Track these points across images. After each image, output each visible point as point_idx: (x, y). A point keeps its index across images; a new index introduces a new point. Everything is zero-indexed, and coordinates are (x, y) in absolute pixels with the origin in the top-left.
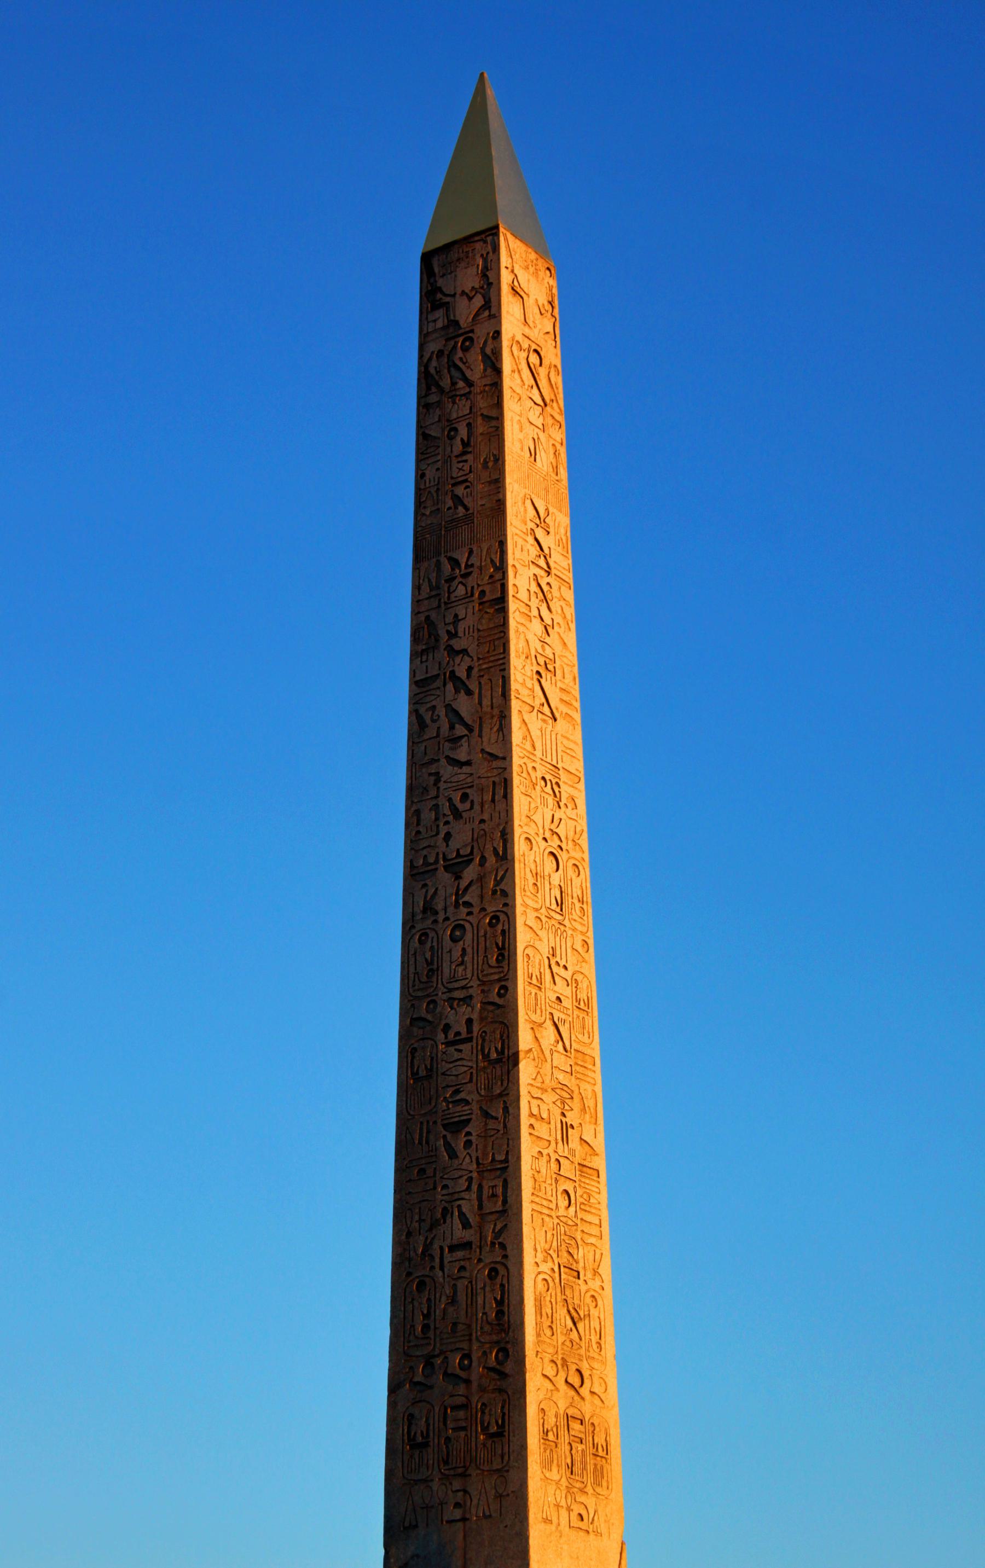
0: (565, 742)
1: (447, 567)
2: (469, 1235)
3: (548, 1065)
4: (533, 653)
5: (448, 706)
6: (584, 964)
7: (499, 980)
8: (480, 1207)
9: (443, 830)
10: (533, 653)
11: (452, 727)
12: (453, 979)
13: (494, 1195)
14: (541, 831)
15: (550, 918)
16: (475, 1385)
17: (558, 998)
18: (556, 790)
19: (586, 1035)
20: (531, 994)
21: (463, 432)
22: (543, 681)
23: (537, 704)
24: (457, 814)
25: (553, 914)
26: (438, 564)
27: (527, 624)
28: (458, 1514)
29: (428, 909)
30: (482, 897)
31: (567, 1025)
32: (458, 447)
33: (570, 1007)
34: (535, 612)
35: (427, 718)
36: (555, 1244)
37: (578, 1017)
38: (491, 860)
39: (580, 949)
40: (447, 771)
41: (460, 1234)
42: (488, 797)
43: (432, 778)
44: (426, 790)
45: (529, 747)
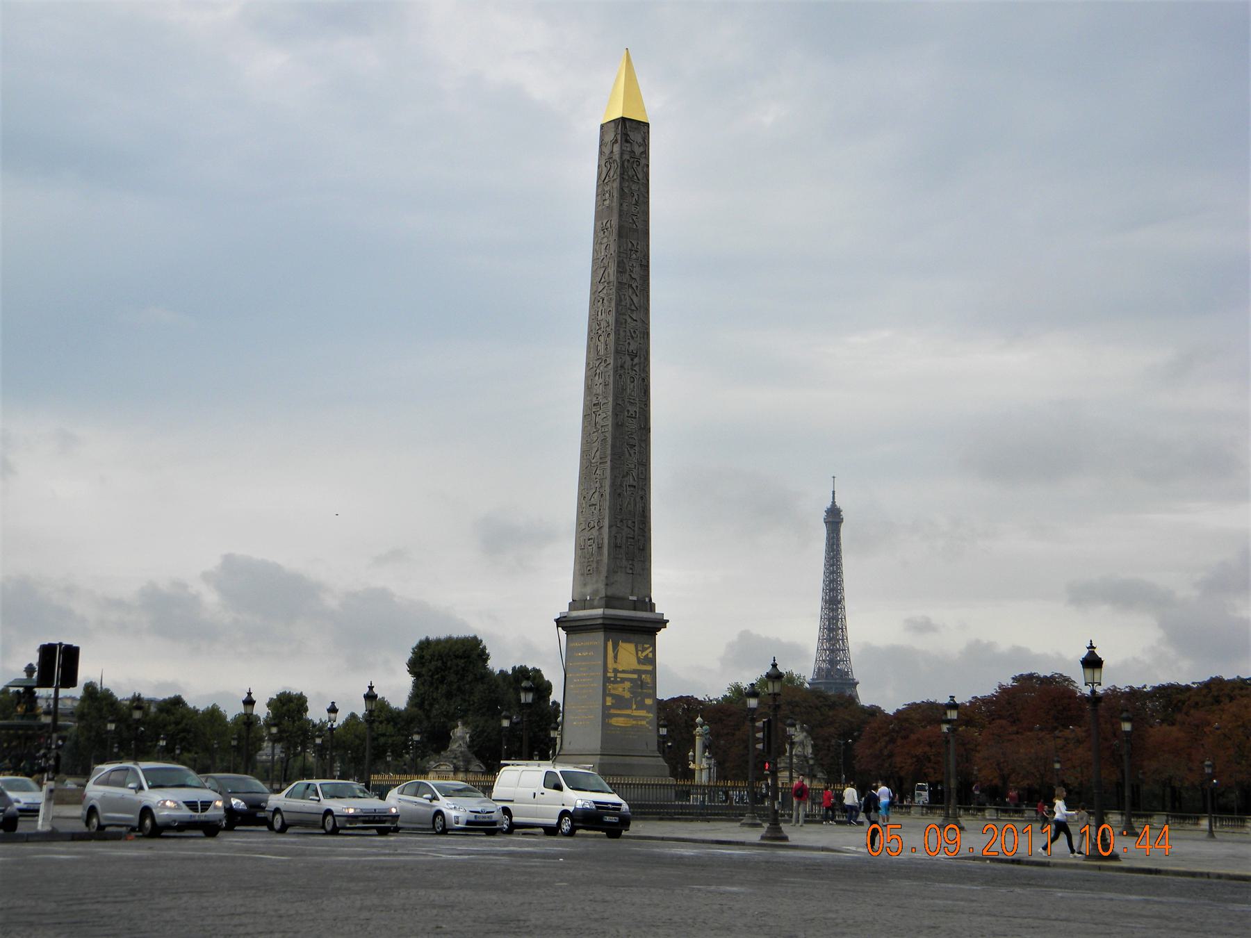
1: (630, 245)
2: (635, 484)
5: (630, 297)
7: (646, 401)
8: (638, 475)
9: (628, 341)
11: (631, 305)
12: (630, 395)
13: (642, 473)
16: (636, 533)
21: (636, 197)
24: (632, 336)
26: (627, 243)
28: (631, 572)
29: (622, 367)
30: (640, 370)
32: (634, 202)
35: (623, 297)
38: (642, 359)
40: (629, 320)
41: (632, 482)
42: (642, 336)
43: (624, 321)
44: (622, 324)
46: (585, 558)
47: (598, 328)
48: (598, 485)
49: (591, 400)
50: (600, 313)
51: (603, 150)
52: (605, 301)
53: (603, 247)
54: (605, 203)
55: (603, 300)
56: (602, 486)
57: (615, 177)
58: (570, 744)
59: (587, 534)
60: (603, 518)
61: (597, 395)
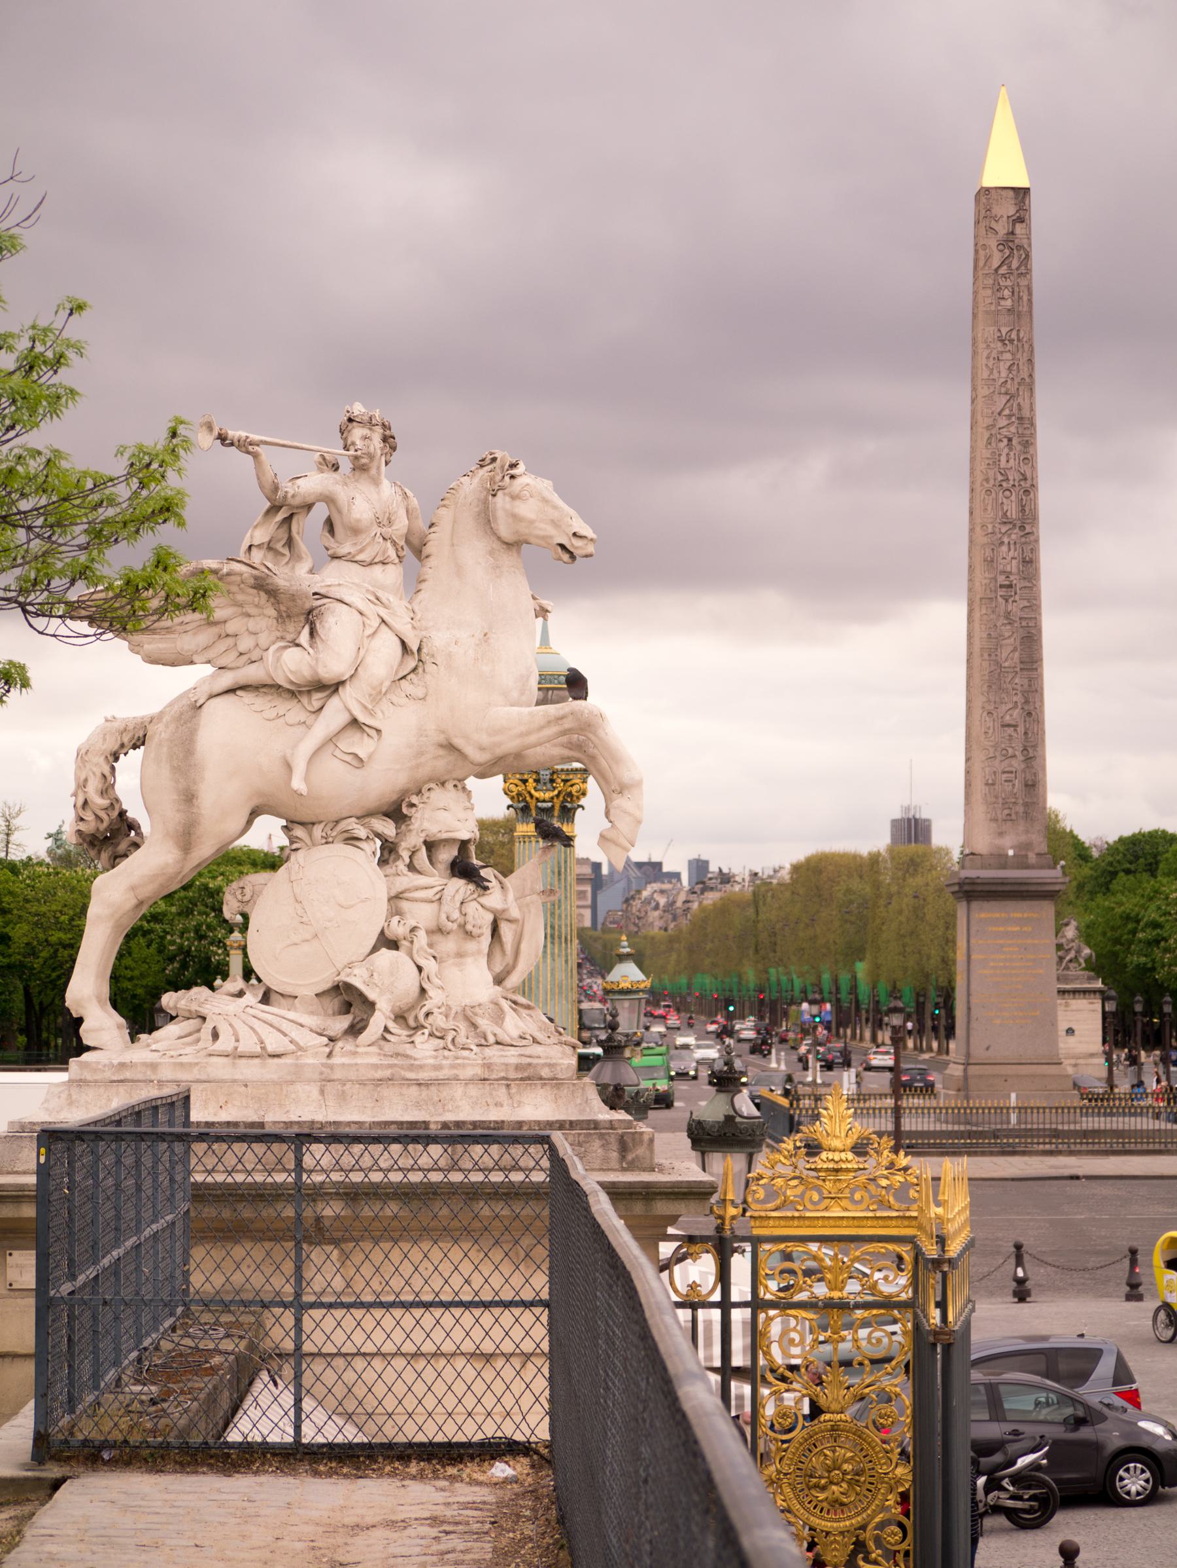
46: (996, 797)
47: (1000, 478)
48: (1019, 698)
49: (995, 579)
50: (1003, 459)
51: (994, 225)
52: (1014, 442)
53: (1003, 367)
54: (1003, 303)
55: (1010, 440)
56: (1027, 702)
57: (1023, 270)
58: (988, 1049)
59: (998, 765)
60: (1035, 747)
61: (1007, 574)
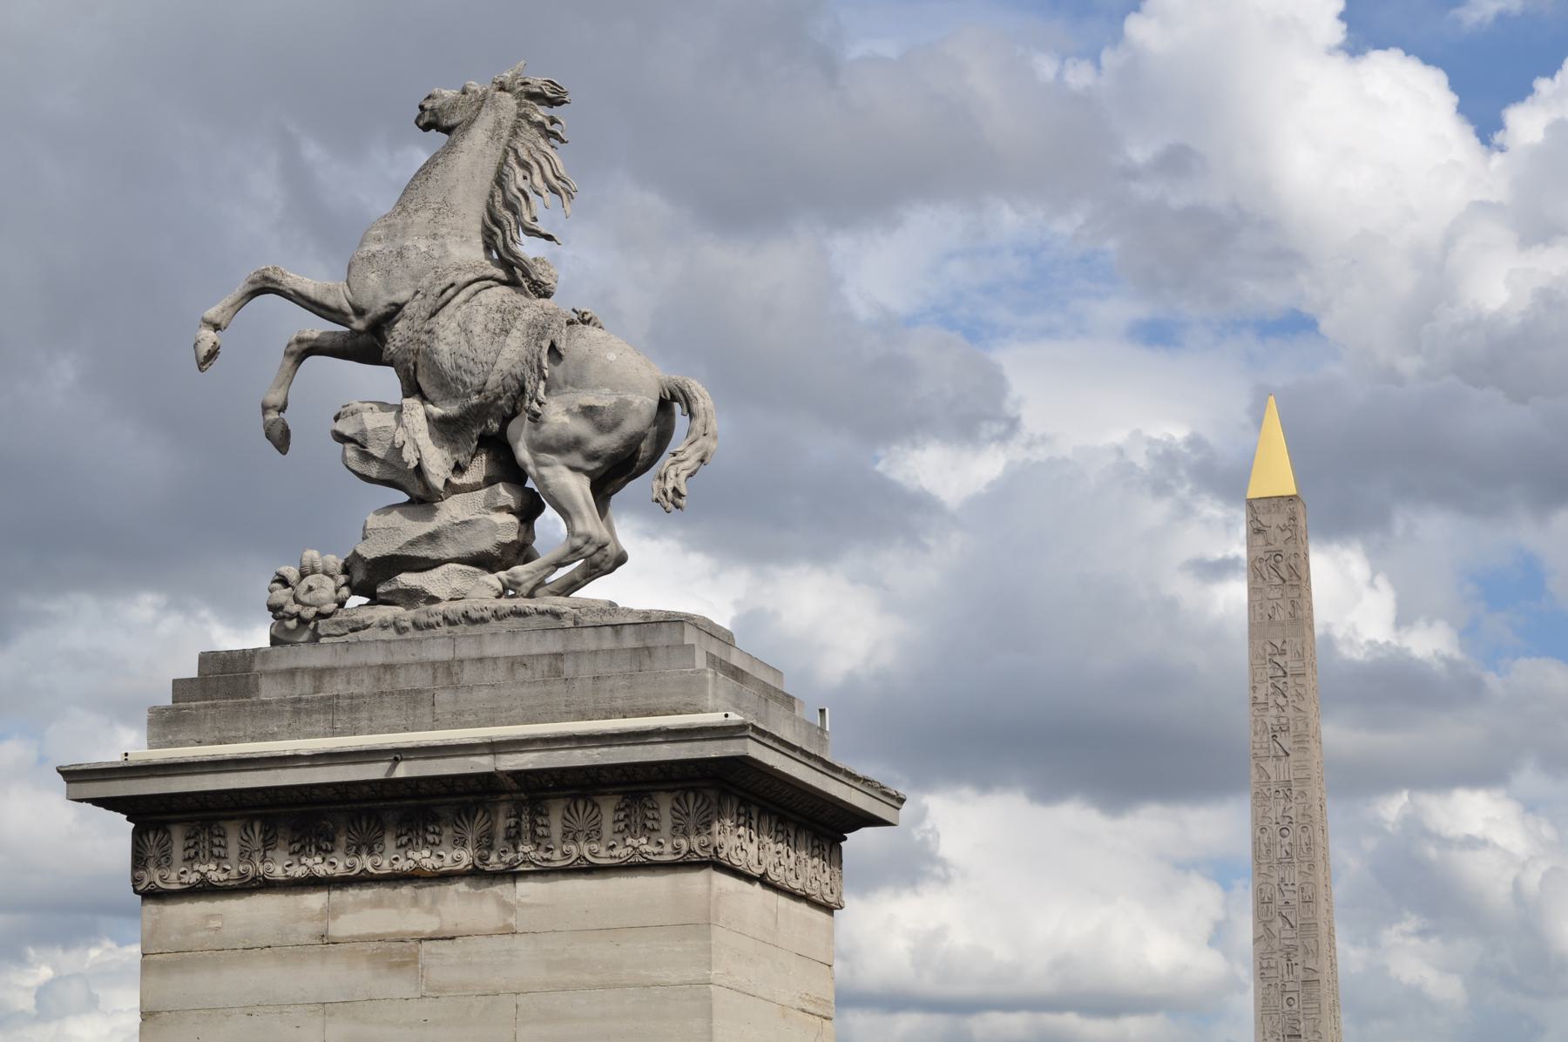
0: (1297, 764)
3: (1277, 940)
4: (1269, 727)
6: (1310, 877)
10: (1269, 727)
14: (1274, 820)
15: (1281, 863)
17: (1286, 903)
18: (1288, 793)
19: (1310, 913)
20: (1263, 907)
22: (1278, 739)
23: (1272, 753)
25: (1284, 860)
27: (1265, 713)
31: (1294, 914)
33: (1297, 903)
34: (1271, 703)
36: (1280, 1026)
37: (1304, 906)
39: (1306, 870)
45: (1264, 779)
